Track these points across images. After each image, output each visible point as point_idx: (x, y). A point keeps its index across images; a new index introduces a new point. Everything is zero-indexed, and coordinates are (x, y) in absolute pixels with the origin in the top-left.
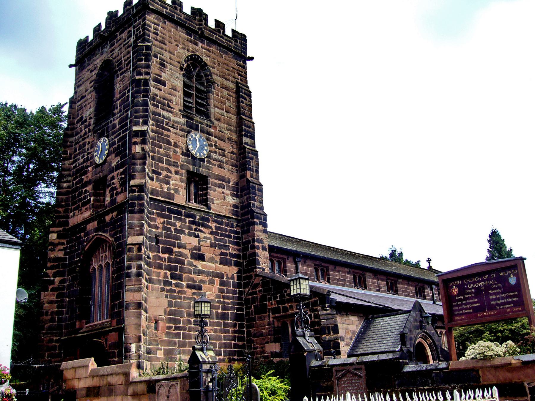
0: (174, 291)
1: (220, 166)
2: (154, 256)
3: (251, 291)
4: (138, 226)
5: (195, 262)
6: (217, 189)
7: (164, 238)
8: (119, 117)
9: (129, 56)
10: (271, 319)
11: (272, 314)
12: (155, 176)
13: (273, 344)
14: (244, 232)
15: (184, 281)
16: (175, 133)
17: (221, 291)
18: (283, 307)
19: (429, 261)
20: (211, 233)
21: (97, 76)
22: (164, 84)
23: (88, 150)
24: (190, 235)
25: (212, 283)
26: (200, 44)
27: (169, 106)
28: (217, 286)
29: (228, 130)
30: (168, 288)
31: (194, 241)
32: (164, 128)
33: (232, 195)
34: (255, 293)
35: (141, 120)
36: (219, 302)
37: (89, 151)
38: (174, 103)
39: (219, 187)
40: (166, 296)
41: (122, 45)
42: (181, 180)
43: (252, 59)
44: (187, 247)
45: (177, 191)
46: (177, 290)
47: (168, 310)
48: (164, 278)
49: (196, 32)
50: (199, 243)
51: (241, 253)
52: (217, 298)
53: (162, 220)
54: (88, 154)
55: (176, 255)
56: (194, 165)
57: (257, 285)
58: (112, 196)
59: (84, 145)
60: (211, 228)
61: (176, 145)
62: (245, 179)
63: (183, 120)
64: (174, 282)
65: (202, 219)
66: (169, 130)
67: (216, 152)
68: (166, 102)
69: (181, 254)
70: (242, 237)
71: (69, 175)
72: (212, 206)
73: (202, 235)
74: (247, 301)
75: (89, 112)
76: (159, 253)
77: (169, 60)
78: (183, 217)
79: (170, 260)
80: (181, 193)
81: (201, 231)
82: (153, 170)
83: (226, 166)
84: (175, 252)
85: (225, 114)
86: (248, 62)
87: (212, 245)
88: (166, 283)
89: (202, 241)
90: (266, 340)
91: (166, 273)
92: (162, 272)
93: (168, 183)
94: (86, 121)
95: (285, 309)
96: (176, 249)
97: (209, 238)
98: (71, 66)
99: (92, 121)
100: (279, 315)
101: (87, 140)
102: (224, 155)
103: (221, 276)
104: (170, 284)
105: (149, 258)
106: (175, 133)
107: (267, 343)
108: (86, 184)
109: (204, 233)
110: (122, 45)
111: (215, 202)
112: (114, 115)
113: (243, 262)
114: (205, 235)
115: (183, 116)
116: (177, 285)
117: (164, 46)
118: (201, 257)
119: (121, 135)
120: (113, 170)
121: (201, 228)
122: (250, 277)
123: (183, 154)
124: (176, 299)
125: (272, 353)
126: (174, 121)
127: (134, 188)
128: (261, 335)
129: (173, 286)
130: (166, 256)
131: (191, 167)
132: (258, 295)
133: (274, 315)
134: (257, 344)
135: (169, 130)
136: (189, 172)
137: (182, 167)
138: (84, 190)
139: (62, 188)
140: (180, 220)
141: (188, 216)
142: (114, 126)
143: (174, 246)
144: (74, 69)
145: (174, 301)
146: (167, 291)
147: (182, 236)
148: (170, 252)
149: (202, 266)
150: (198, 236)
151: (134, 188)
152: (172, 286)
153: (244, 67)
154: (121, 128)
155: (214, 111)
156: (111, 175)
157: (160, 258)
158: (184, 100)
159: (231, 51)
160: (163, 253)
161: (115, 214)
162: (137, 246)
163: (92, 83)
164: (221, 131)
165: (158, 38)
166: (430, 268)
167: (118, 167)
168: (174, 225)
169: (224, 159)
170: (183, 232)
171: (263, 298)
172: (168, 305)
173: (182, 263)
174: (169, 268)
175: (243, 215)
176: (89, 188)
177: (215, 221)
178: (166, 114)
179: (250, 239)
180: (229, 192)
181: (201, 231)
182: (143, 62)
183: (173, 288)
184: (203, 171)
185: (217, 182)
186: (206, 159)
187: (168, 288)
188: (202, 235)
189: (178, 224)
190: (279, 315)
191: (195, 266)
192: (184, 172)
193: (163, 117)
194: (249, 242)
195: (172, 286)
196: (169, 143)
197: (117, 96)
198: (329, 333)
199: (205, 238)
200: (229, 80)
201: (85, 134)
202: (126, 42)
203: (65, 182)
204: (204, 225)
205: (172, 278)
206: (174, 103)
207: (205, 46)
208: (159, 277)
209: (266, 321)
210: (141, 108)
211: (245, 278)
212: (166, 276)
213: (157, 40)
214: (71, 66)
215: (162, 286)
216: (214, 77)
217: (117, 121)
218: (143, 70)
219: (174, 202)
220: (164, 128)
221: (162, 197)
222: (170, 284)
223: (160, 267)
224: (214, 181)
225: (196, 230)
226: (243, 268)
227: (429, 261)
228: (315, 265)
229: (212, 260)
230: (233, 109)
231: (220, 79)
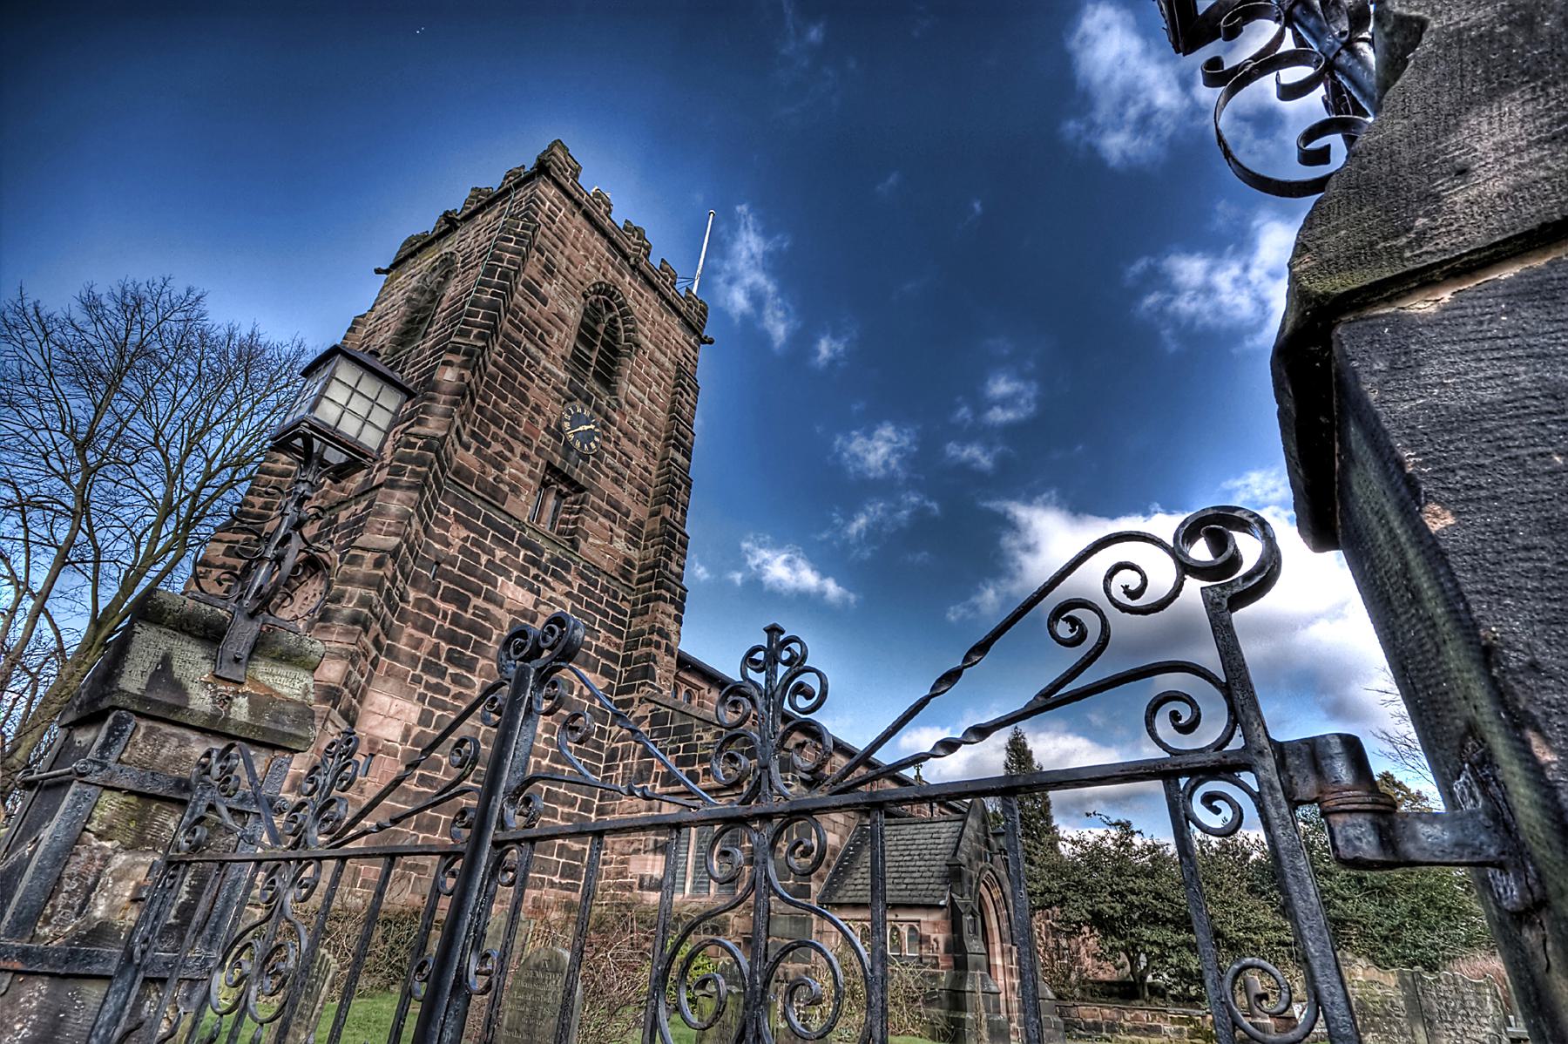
0: (447, 692)
1: (615, 481)
2: (418, 600)
4: (397, 516)
6: (601, 519)
12: (474, 444)
15: (480, 676)
16: (541, 388)
20: (568, 595)
22: (544, 302)
24: (520, 583)
26: (628, 278)
27: (541, 337)
29: (645, 428)
30: (434, 680)
31: (524, 598)
32: (521, 370)
36: (548, 742)
38: (555, 340)
39: (605, 516)
40: (422, 698)
42: (531, 475)
44: (506, 605)
45: (515, 490)
46: (455, 689)
47: (416, 730)
48: (430, 654)
49: (626, 257)
50: (536, 606)
51: (621, 654)
53: (464, 533)
55: (474, 614)
56: (566, 458)
60: (569, 584)
61: (537, 409)
62: (659, 518)
64: (451, 670)
65: (556, 561)
66: (532, 380)
67: (614, 455)
68: (539, 331)
69: (487, 616)
72: (582, 544)
76: (435, 597)
77: (564, 270)
78: (514, 544)
79: (456, 620)
80: (523, 498)
81: (547, 584)
82: (473, 432)
83: (628, 486)
84: (475, 607)
85: (647, 401)
88: (429, 667)
89: (545, 604)
90: (636, 845)
91: (437, 646)
92: (430, 640)
93: (500, 468)
96: (478, 602)
97: (561, 604)
102: (628, 466)
104: (442, 673)
105: (403, 598)
106: (541, 388)
107: (637, 851)
109: (554, 590)
111: (590, 540)
114: (554, 595)
115: (566, 369)
116: (456, 679)
117: (560, 245)
121: (549, 579)
123: (547, 429)
124: (445, 710)
125: (642, 878)
126: (545, 368)
127: (413, 440)
129: (448, 678)
130: (451, 608)
131: (558, 461)
135: (532, 380)
136: (550, 466)
140: (507, 547)
141: (525, 544)
143: (478, 595)
145: (439, 713)
146: (428, 686)
147: (500, 579)
148: (463, 603)
150: (538, 593)
152: (443, 679)
155: (626, 388)
157: (434, 610)
158: (575, 346)
159: (679, 314)
160: (443, 599)
165: (554, 228)
168: (491, 552)
172: (420, 719)
174: (451, 638)
177: (582, 576)
178: (533, 349)
180: (623, 533)
181: (547, 584)
183: (447, 682)
185: (604, 505)
186: (592, 458)
187: (434, 680)
189: (500, 553)
193: (525, 350)
195: (443, 679)
196: (525, 400)
197: (444, 305)
199: (551, 599)
205: (449, 659)
206: (555, 340)
207: (636, 285)
208: (417, 649)
212: (435, 651)
213: (550, 229)
215: (417, 672)
219: (504, 508)
220: (521, 370)
222: (442, 673)
223: (426, 627)
224: (597, 501)
225: (536, 577)
231: (650, 346)
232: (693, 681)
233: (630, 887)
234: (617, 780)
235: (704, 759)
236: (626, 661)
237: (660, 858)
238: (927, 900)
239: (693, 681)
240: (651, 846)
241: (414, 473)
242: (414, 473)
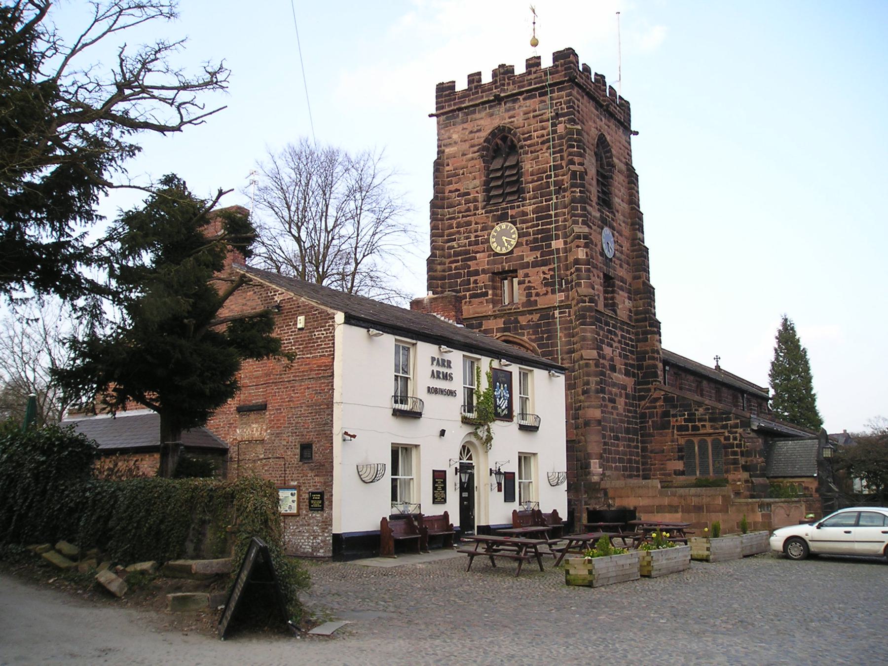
1: (621, 266)
3: (648, 404)
8: (534, 204)
9: (544, 132)
10: (676, 437)
11: (678, 431)
13: (677, 462)
14: (638, 341)
17: (626, 404)
18: (692, 426)
19: (717, 359)
21: (485, 142)
23: (476, 231)
25: (621, 396)
28: (623, 400)
29: (624, 222)
33: (630, 299)
34: (655, 407)
35: (580, 220)
37: (479, 233)
41: (531, 115)
43: (636, 133)
45: (598, 295)
52: (624, 411)
54: (476, 236)
57: (656, 400)
58: (529, 295)
59: (469, 224)
63: (598, 215)
70: (637, 345)
71: (443, 256)
72: (618, 312)
73: (615, 345)
74: (643, 416)
75: (473, 184)
86: (632, 136)
90: (668, 457)
94: (468, 194)
95: (696, 428)
98: (431, 116)
99: (480, 197)
100: (687, 433)
101: (472, 219)
103: (624, 387)
107: (670, 460)
108: (476, 273)
110: (531, 115)
112: (524, 199)
113: (638, 373)
115: (599, 210)
118: (613, 368)
119: (540, 227)
120: (526, 266)
122: (649, 390)
127: (584, 298)
128: (663, 451)
132: (659, 410)
133: (679, 433)
134: (655, 460)
136: (605, 275)
137: (601, 269)
138: (472, 279)
139: (436, 271)
142: (525, 214)
144: (435, 118)
149: (617, 378)
150: (612, 346)
151: (584, 298)
153: (629, 144)
154: (538, 219)
156: (526, 271)
161: (536, 317)
162: (594, 362)
163: (476, 149)
164: (620, 225)
166: (718, 367)
167: (535, 264)
169: (623, 257)
171: (666, 414)
175: (637, 321)
176: (484, 279)
179: (648, 349)
180: (626, 295)
182: (575, 149)
190: (687, 433)
192: (601, 275)
194: (646, 352)
198: (755, 456)
200: (621, 161)
201: (468, 210)
202: (537, 113)
203: (440, 264)
207: (606, 121)
209: (668, 438)
210: (579, 205)
211: (640, 390)
214: (431, 116)
216: (614, 159)
217: (531, 208)
218: (576, 159)
226: (638, 379)
227: (717, 359)
228: (675, 373)
229: (620, 372)
230: (626, 197)
233: (670, 475)
234: (649, 428)
235: (700, 420)
236: (640, 367)
237: (681, 462)
238: (808, 475)
240: (677, 457)
241: (591, 317)
242: (591, 317)
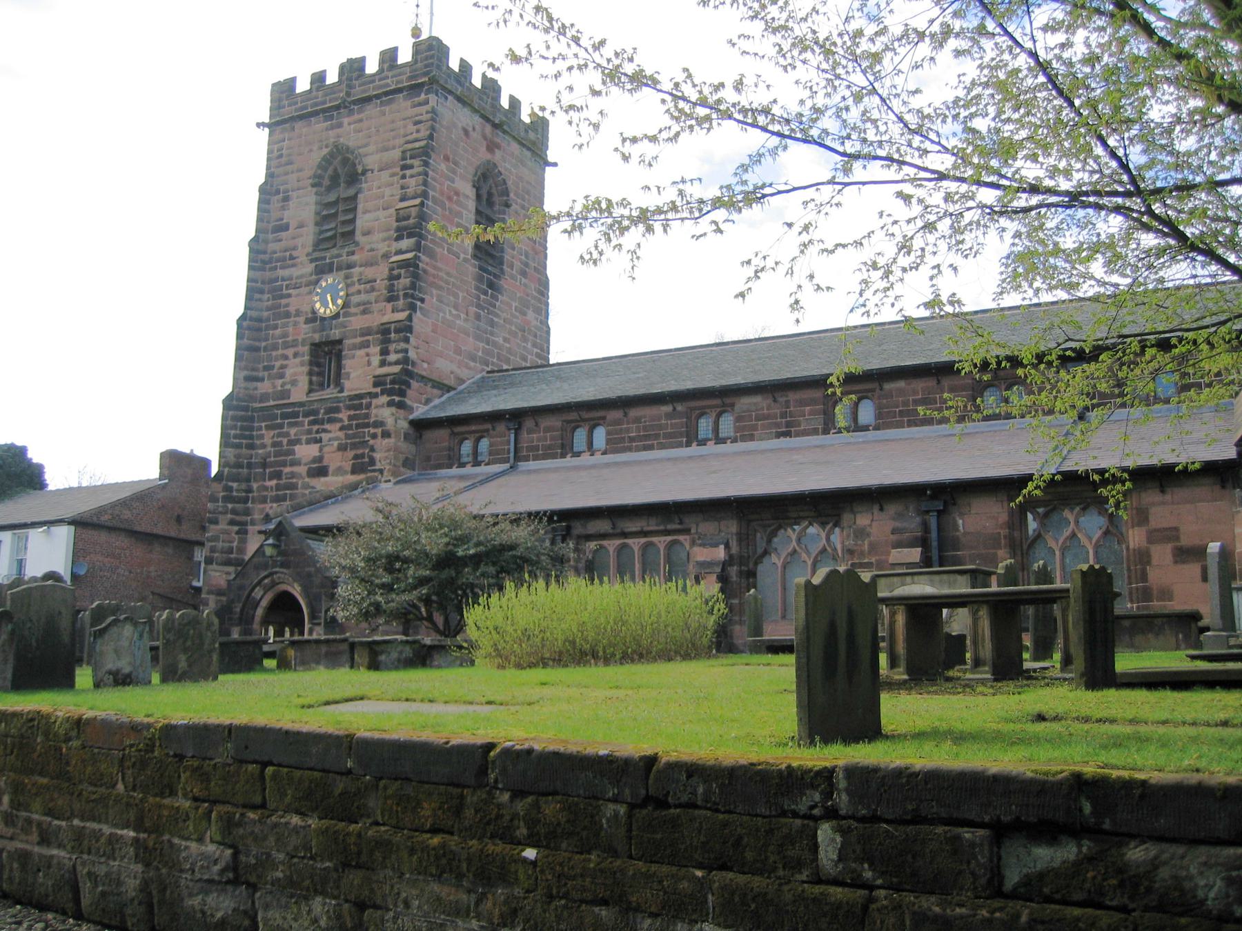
5: (315, 482)
7: (272, 459)
20: (341, 429)
24: (308, 442)
39: (360, 348)
44: (303, 461)
53: (272, 433)
60: (341, 420)
69: (293, 475)
79: (278, 488)
81: (325, 431)
87: (342, 448)
96: (287, 470)
118: (322, 472)
130: (274, 482)
141: (306, 415)
148: (278, 475)
157: (266, 488)
168: (287, 434)
170: (298, 442)
173: (293, 487)
184: (336, 334)
185: (359, 340)
188: (325, 436)
189: (293, 431)
191: (313, 488)
204: (330, 421)
219: (292, 400)
221: (274, 400)
229: (339, 471)
232: (474, 428)
239: (474, 428)
